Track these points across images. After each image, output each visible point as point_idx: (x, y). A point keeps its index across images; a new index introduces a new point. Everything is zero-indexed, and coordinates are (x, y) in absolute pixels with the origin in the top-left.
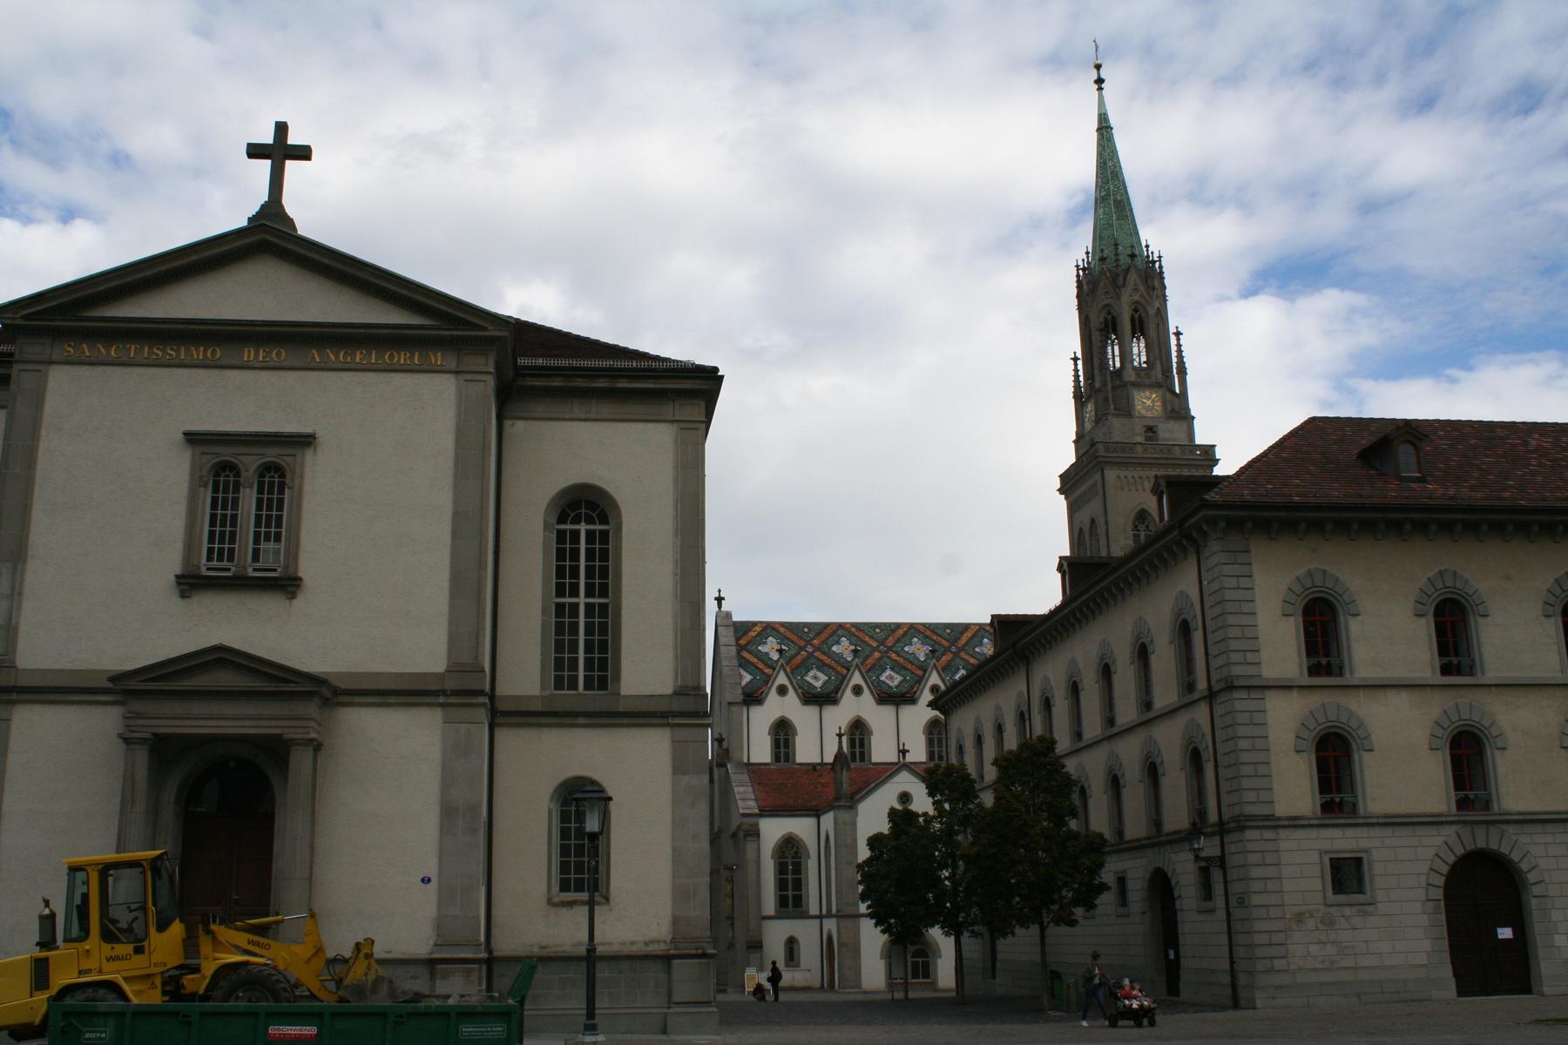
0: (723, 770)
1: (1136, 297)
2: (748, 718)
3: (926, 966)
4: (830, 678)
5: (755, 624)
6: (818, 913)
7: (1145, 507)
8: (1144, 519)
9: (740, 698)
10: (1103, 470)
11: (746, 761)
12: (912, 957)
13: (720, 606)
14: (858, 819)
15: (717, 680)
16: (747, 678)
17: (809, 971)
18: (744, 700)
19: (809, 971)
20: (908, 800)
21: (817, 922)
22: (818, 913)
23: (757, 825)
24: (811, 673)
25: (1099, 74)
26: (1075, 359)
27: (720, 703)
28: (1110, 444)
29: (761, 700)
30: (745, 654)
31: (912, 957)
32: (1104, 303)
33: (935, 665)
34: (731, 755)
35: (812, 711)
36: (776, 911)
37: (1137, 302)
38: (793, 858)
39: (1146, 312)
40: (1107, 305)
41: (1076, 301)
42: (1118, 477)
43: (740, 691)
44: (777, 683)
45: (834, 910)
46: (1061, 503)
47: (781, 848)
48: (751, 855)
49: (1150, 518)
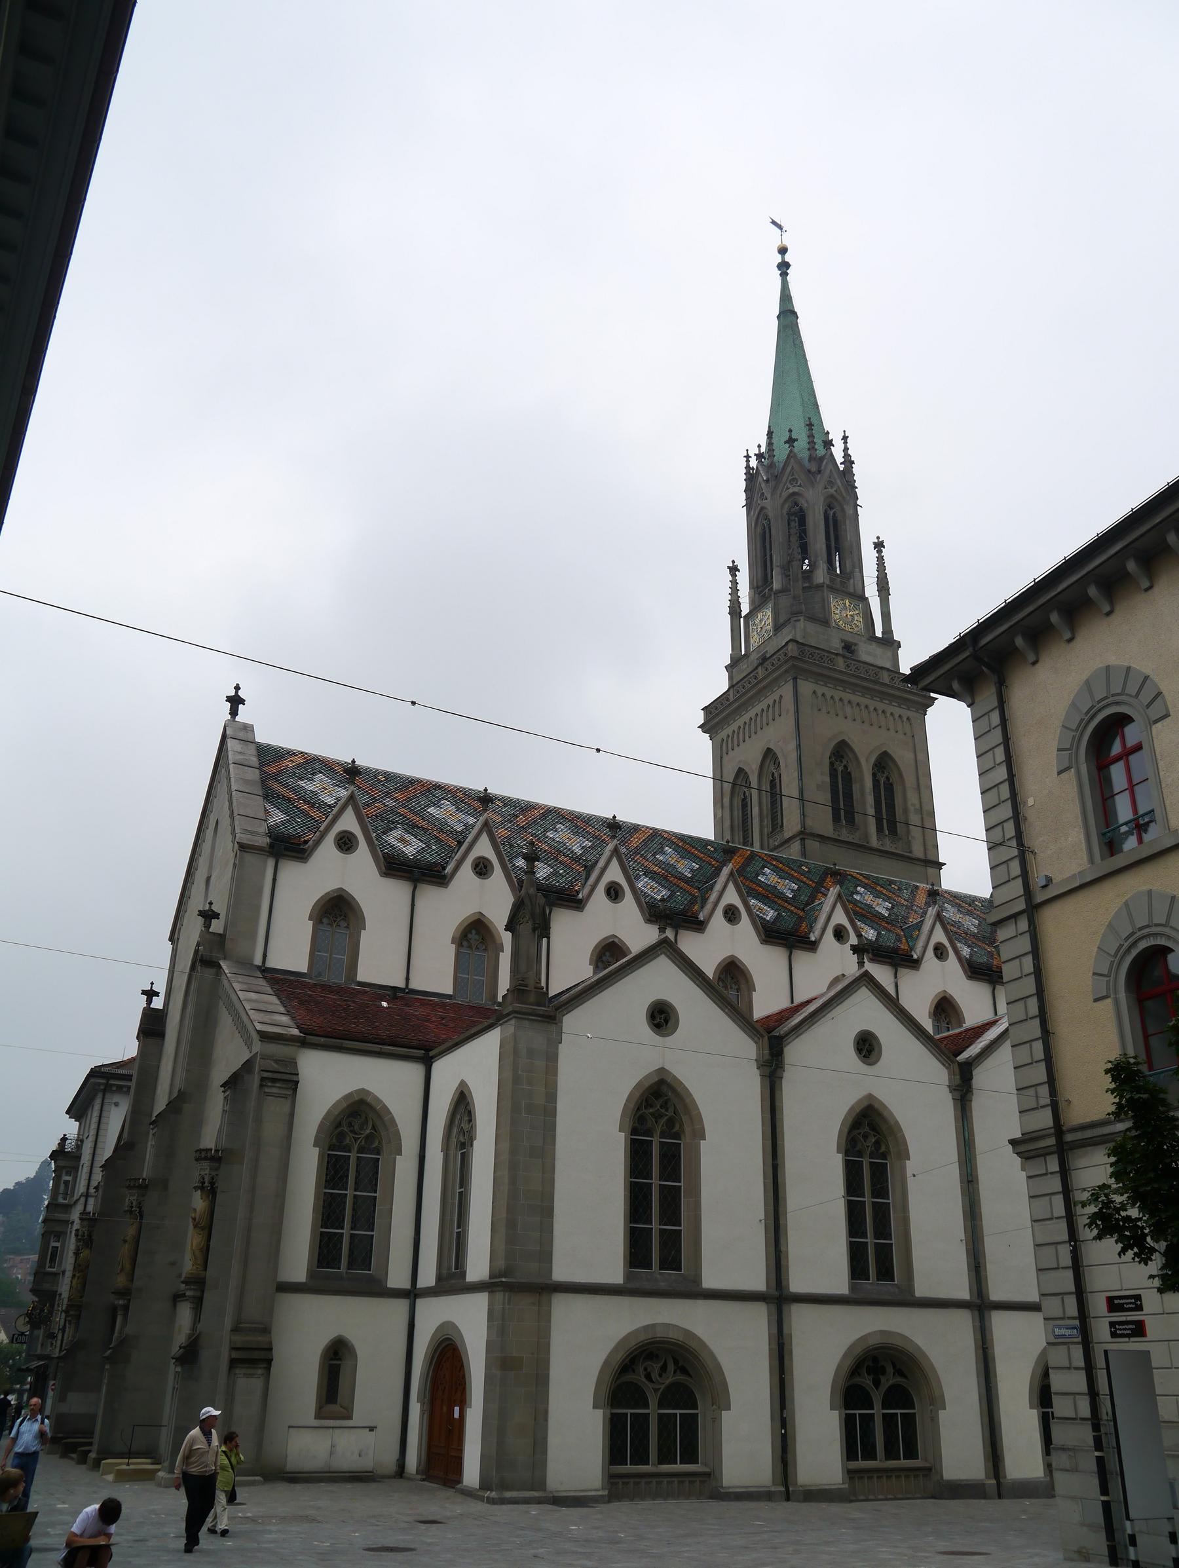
0: (209, 973)
1: (832, 491)
2: (274, 880)
3: (690, 1424)
4: (428, 846)
5: (291, 753)
6: (406, 1285)
7: (847, 739)
8: (842, 757)
9: (264, 841)
10: (795, 679)
11: (258, 961)
12: (660, 1406)
13: (234, 712)
14: (563, 1049)
15: (209, 833)
16: (277, 817)
17: (372, 1429)
18: (271, 846)
19: (372, 1429)
20: (666, 1021)
21: (402, 1305)
22: (406, 1285)
23: (293, 1063)
24: (397, 833)
25: (783, 258)
26: (734, 570)
27: (208, 879)
28: (806, 648)
29: (304, 851)
30: (276, 786)
31: (660, 1406)
32: (791, 491)
33: (616, 851)
34: (228, 945)
35: (396, 891)
36: (311, 1274)
37: (832, 496)
38: (361, 1150)
39: (843, 510)
40: (794, 494)
41: (744, 496)
42: (814, 692)
43: (263, 829)
44: (340, 826)
45: (478, 1267)
46: (705, 743)
47: (339, 1124)
48: (272, 1129)
49: (851, 755)
